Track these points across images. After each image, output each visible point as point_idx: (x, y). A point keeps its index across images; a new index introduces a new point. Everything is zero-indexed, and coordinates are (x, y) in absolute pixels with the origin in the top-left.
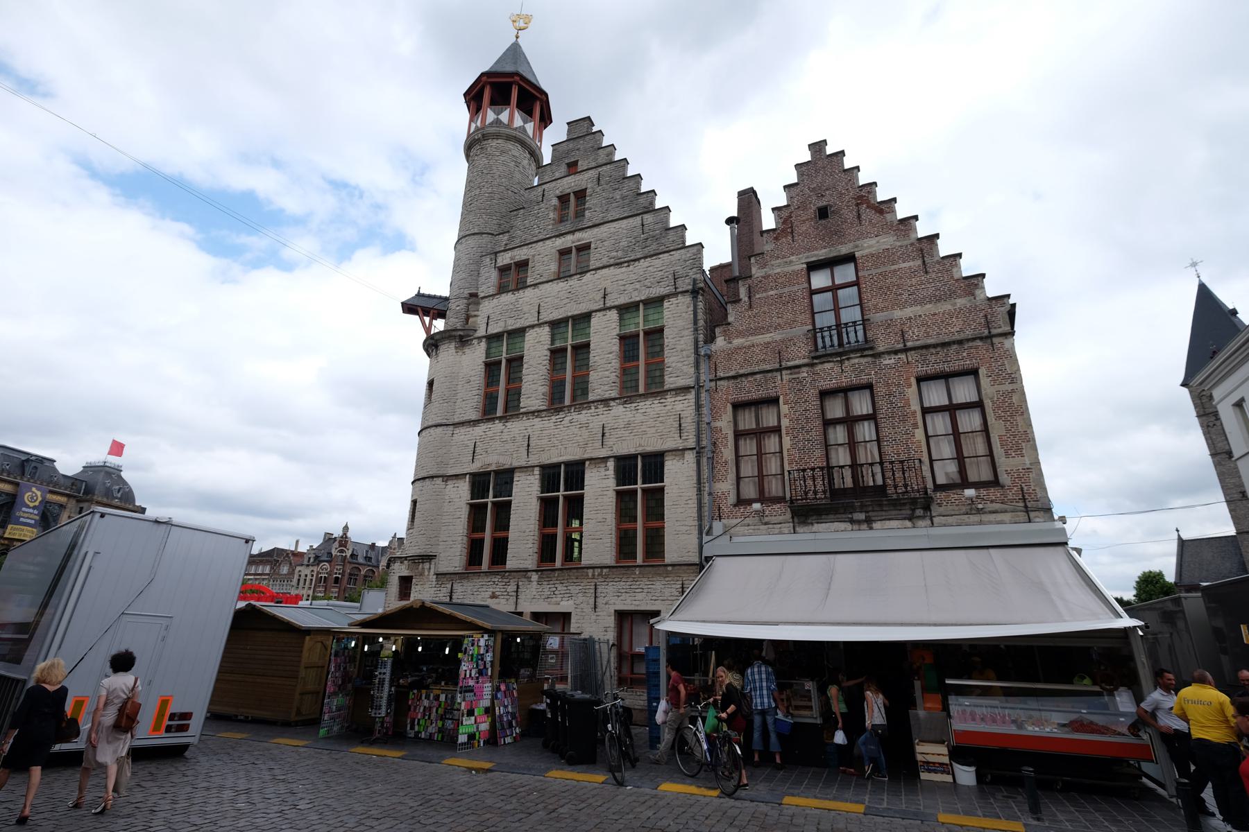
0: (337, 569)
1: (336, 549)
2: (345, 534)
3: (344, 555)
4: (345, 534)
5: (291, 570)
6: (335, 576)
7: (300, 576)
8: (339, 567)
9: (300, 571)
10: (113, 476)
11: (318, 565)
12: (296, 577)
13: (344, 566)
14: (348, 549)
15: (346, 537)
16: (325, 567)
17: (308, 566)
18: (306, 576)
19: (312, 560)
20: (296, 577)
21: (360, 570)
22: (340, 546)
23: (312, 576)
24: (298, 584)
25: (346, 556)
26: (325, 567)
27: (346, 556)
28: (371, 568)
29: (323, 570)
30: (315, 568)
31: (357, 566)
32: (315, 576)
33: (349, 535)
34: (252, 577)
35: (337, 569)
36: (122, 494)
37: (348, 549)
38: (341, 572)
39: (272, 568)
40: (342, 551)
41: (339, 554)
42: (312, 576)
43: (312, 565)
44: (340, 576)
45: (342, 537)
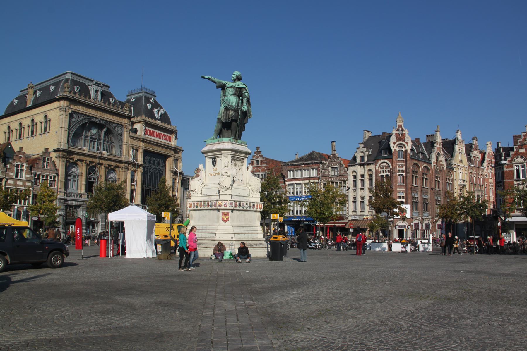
0: (399, 166)
1: (395, 143)
5: (343, 172)
6: (398, 174)
7: (355, 177)
8: (401, 164)
10: (151, 100)
12: (351, 178)
13: (406, 162)
14: (407, 143)
16: (384, 164)
18: (362, 176)
19: (366, 159)
20: (351, 178)
21: (419, 167)
22: (398, 140)
23: (370, 175)
24: (355, 186)
25: (406, 151)
26: (384, 164)
27: (406, 151)
28: (426, 165)
29: (382, 168)
30: (372, 167)
31: (416, 162)
32: (374, 175)
34: (300, 182)
35: (399, 166)
36: (161, 115)
37: (407, 143)
38: (404, 169)
39: (318, 171)
40: (401, 146)
41: (397, 149)
43: (368, 164)
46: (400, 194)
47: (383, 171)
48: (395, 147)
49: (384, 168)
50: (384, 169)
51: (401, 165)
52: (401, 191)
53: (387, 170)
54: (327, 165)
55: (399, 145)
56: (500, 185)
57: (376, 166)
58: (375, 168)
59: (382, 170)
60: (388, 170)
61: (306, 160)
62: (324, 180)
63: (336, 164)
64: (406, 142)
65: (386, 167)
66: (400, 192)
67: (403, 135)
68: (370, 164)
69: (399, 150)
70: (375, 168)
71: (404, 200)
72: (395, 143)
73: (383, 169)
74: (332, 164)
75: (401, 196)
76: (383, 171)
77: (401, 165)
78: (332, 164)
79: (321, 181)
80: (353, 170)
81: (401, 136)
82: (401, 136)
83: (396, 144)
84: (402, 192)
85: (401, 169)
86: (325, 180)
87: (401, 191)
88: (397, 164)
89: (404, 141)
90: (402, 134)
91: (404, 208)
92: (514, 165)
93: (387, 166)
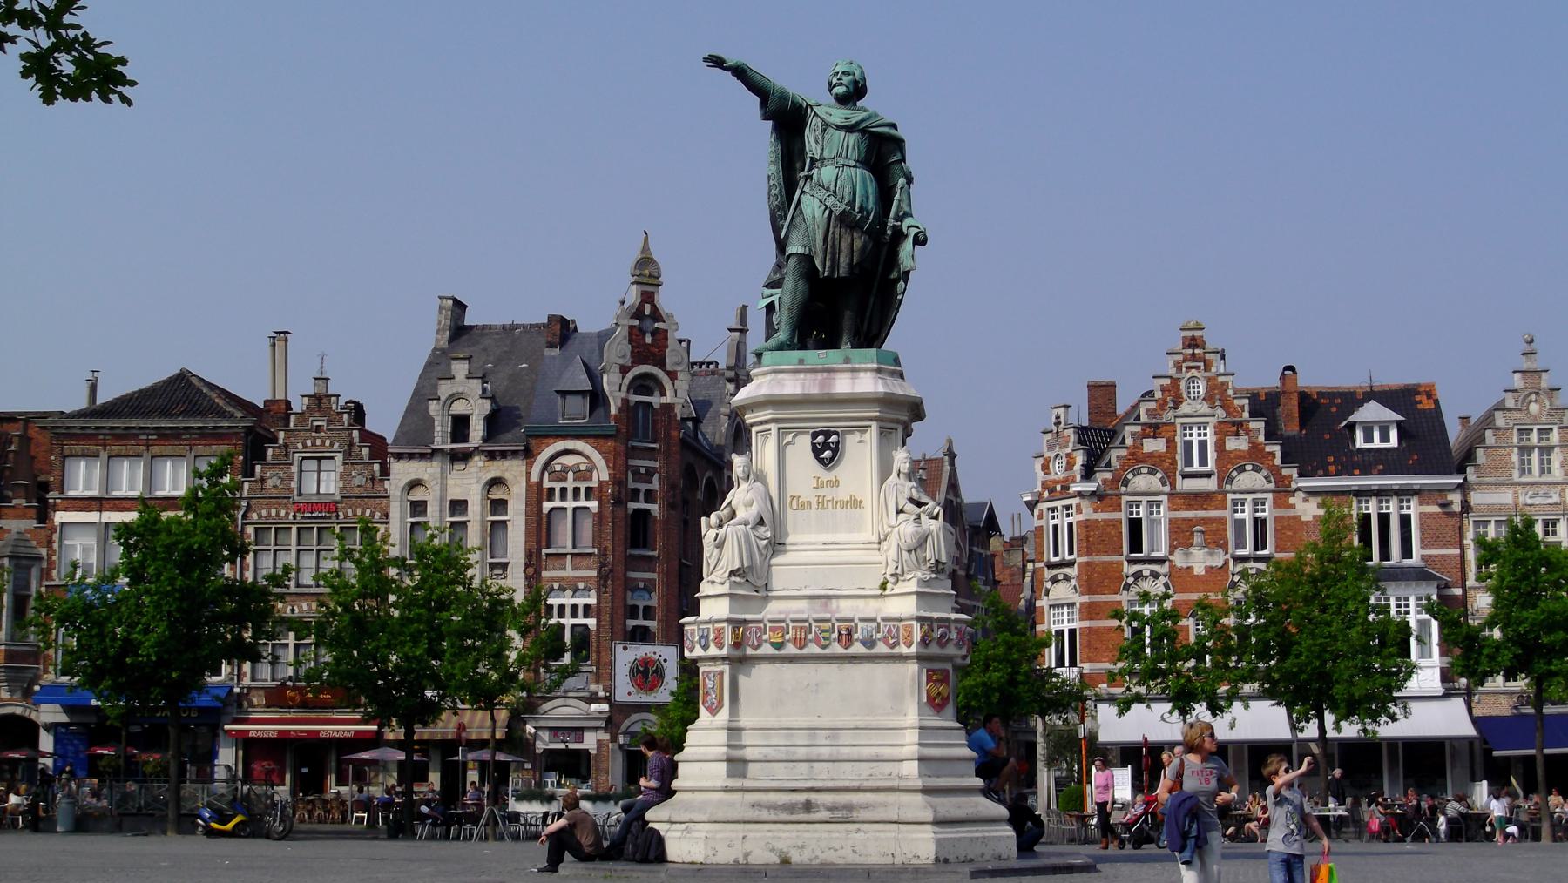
2: (648, 297)
3: (656, 400)
4: (648, 297)
6: (632, 506)
7: (418, 507)
8: (643, 464)
9: (414, 484)
11: (528, 454)
14: (673, 376)
15: (656, 315)
16: (570, 460)
17: (463, 457)
18: (459, 506)
19: (477, 430)
30: (512, 470)
33: (666, 300)
35: (636, 472)
37: (673, 376)
42: (499, 506)
44: (654, 508)
45: (638, 314)
46: (636, 594)
47: (564, 490)
48: (624, 388)
49: (570, 475)
50: (570, 484)
51: (643, 470)
52: (641, 585)
53: (583, 486)
54: (281, 442)
55: (639, 382)
56: (1061, 577)
57: (530, 465)
58: (528, 474)
59: (558, 486)
60: (588, 489)
61: (165, 413)
62: (264, 513)
63: (328, 443)
64: (669, 368)
65: (581, 475)
66: (638, 588)
67: (658, 337)
68: (504, 455)
69: (638, 403)
70: (528, 474)
71: (652, 624)
72: (624, 370)
73: (565, 479)
74: (309, 443)
75: (641, 604)
76: (564, 490)
77: (643, 470)
78: (309, 443)
79: (245, 516)
80: (413, 477)
81: (649, 340)
82: (649, 340)
83: (630, 375)
84: (645, 588)
85: (643, 487)
86: (269, 515)
87: (641, 585)
88: (633, 462)
89: (661, 364)
90: (653, 334)
91: (657, 657)
92: (1125, 499)
93: (583, 468)
